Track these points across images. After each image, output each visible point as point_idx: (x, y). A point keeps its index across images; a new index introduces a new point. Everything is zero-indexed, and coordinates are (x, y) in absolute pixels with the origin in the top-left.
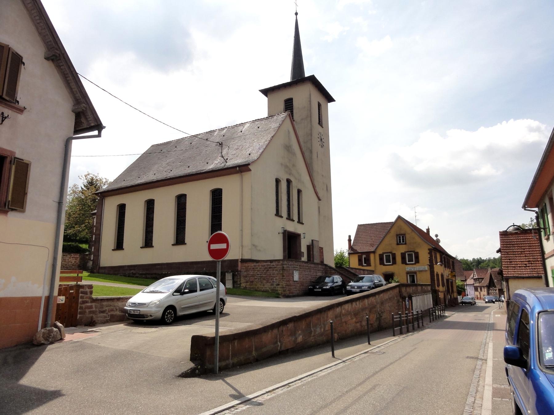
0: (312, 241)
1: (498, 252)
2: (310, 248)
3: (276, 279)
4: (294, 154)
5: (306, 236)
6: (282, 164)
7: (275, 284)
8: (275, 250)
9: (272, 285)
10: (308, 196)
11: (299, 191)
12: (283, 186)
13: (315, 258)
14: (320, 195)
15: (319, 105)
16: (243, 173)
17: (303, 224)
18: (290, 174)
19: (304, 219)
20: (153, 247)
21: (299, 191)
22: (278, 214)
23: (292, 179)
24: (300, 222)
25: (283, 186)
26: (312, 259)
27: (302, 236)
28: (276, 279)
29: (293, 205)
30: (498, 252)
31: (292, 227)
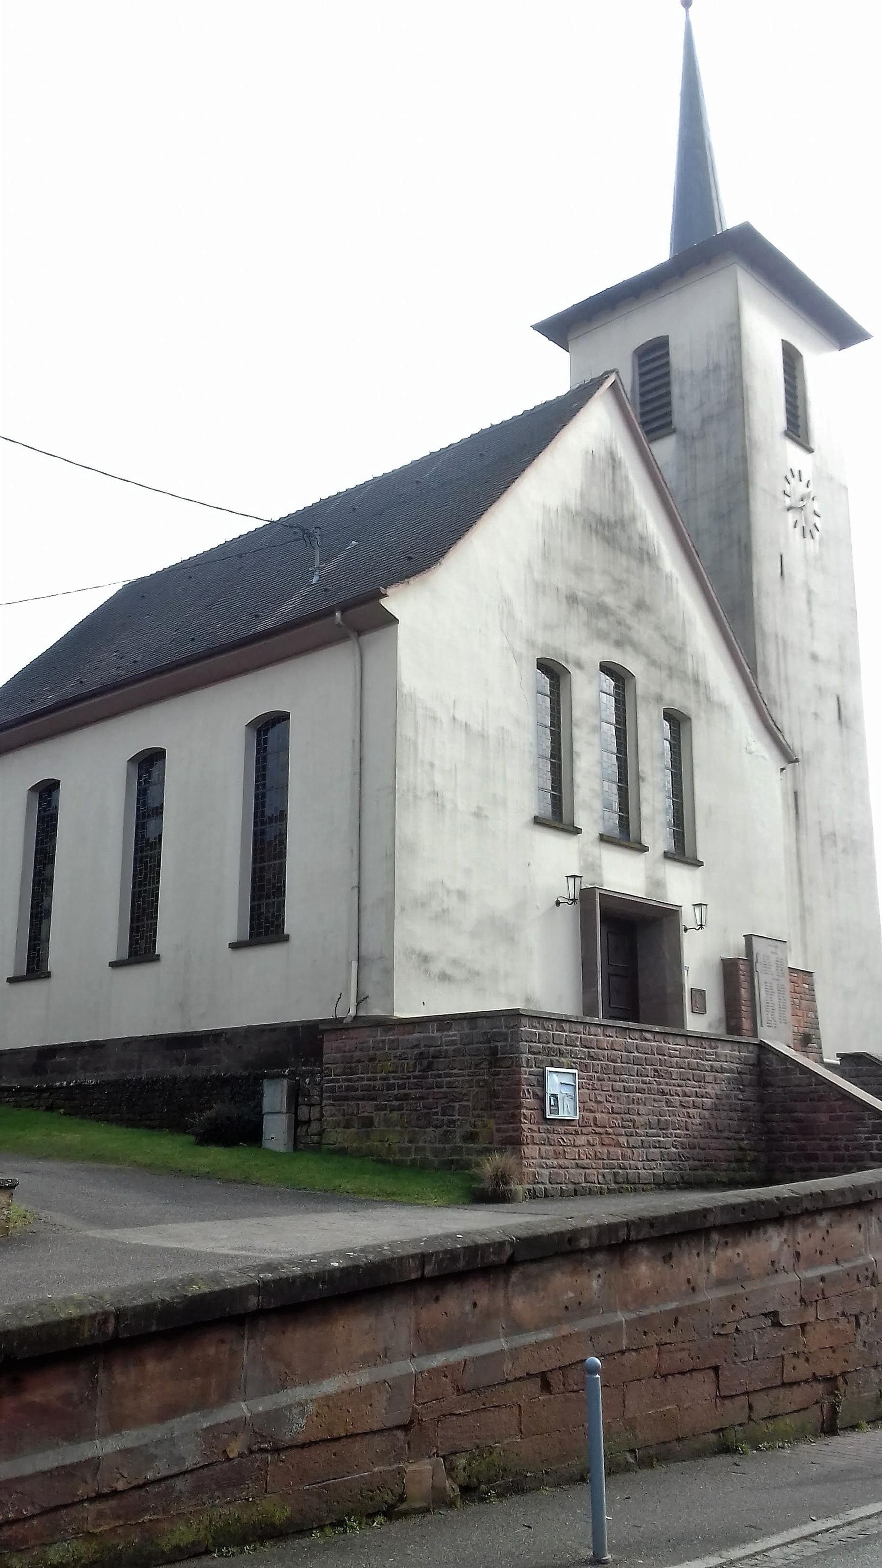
0: (749, 938)
1: (838, 1055)
2: (736, 974)
3: (464, 1110)
4: (645, 556)
5: (713, 915)
6: (572, 599)
7: (459, 1132)
8: (536, 973)
9: (446, 1137)
10: (729, 740)
11: (677, 722)
12: (590, 694)
13: (765, 1015)
14: (793, 739)
15: (791, 359)
16: (365, 638)
17: (699, 864)
18: (618, 644)
19: (705, 845)
20: (157, 958)
21: (677, 722)
22: (557, 817)
23: (633, 664)
24: (682, 852)
25: (590, 694)
26: (746, 1024)
27: (688, 917)
28: (464, 1110)
29: (638, 777)
30: (838, 1055)
31: (626, 876)
